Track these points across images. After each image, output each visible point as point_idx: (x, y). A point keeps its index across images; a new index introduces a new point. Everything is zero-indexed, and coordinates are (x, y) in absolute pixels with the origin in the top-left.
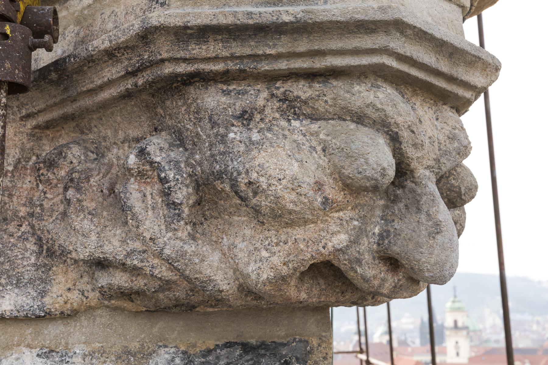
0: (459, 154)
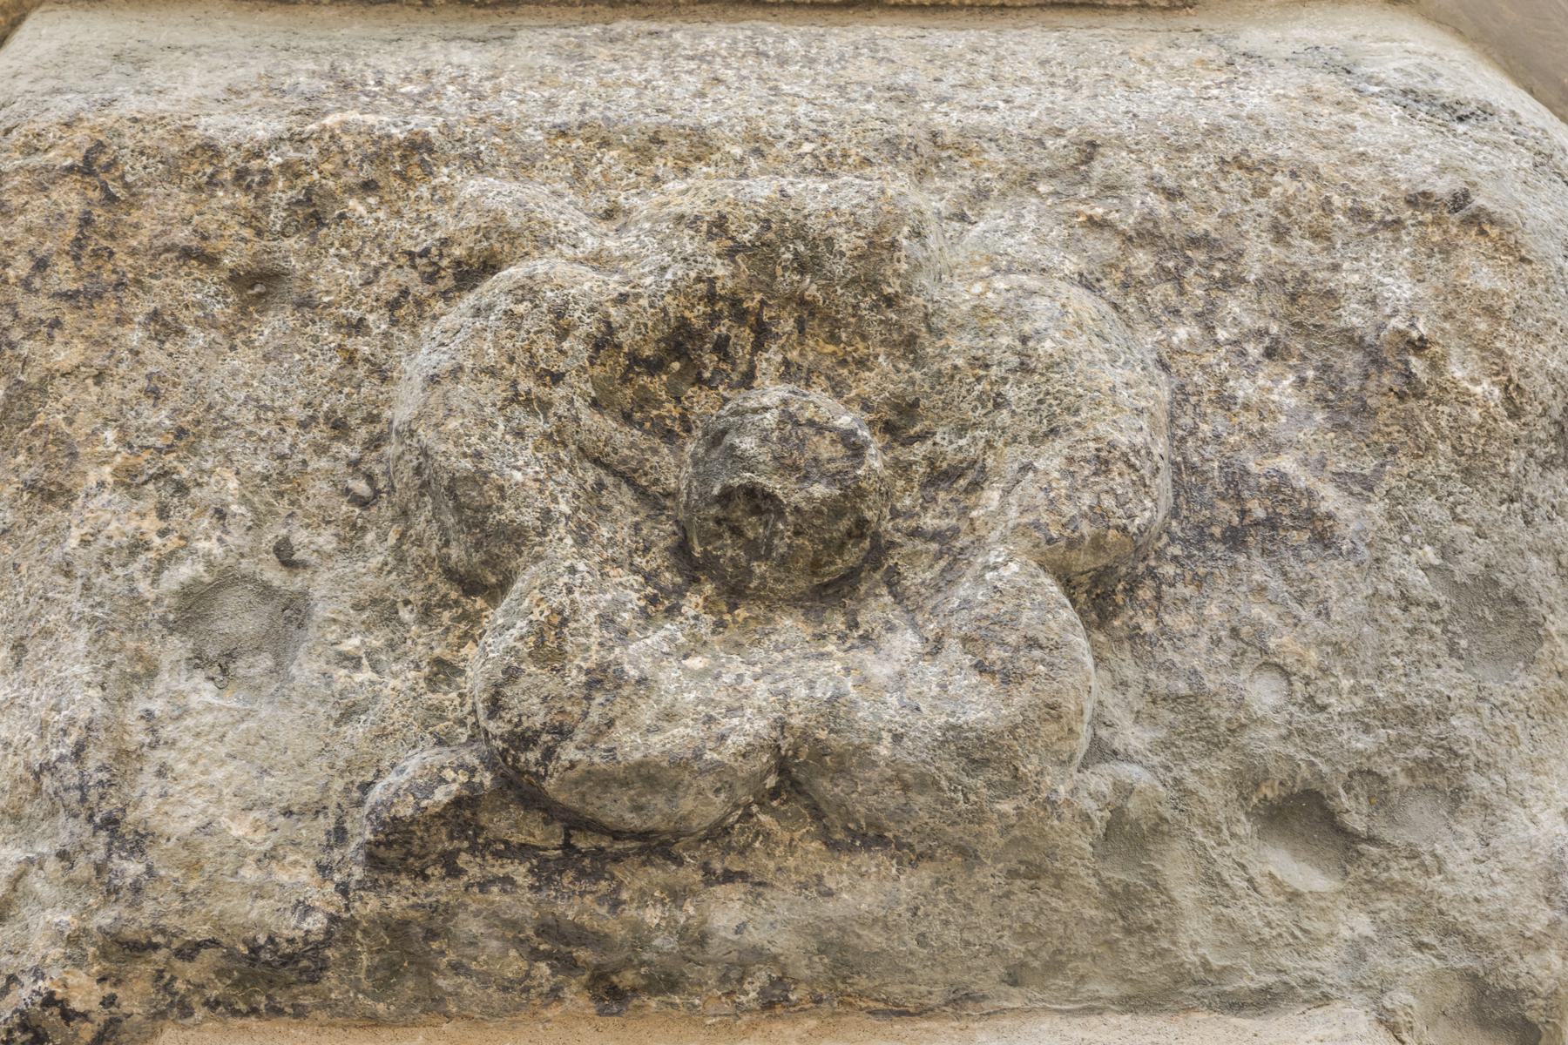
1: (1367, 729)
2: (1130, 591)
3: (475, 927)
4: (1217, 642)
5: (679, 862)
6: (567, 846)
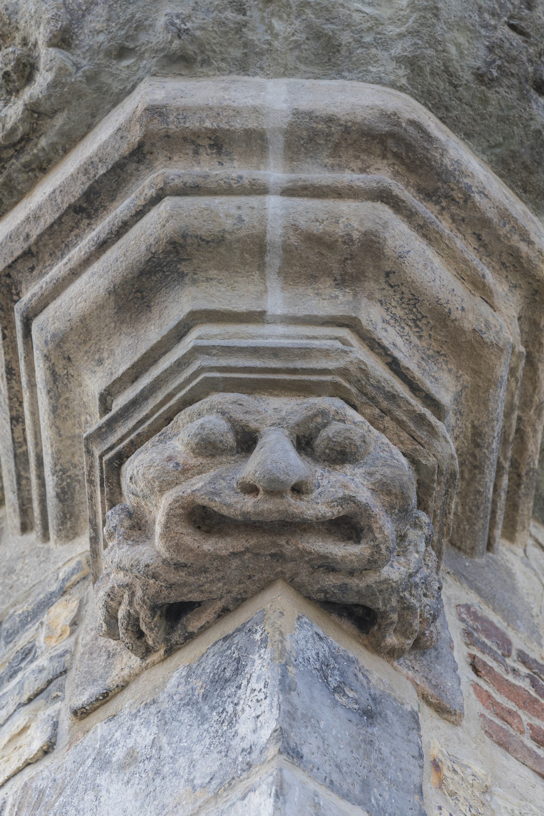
0: (306, 409)
1: (123, 29)
2: (72, 39)
3: (15, 175)
4: (89, 36)
5: (32, 139)
6: (16, 151)
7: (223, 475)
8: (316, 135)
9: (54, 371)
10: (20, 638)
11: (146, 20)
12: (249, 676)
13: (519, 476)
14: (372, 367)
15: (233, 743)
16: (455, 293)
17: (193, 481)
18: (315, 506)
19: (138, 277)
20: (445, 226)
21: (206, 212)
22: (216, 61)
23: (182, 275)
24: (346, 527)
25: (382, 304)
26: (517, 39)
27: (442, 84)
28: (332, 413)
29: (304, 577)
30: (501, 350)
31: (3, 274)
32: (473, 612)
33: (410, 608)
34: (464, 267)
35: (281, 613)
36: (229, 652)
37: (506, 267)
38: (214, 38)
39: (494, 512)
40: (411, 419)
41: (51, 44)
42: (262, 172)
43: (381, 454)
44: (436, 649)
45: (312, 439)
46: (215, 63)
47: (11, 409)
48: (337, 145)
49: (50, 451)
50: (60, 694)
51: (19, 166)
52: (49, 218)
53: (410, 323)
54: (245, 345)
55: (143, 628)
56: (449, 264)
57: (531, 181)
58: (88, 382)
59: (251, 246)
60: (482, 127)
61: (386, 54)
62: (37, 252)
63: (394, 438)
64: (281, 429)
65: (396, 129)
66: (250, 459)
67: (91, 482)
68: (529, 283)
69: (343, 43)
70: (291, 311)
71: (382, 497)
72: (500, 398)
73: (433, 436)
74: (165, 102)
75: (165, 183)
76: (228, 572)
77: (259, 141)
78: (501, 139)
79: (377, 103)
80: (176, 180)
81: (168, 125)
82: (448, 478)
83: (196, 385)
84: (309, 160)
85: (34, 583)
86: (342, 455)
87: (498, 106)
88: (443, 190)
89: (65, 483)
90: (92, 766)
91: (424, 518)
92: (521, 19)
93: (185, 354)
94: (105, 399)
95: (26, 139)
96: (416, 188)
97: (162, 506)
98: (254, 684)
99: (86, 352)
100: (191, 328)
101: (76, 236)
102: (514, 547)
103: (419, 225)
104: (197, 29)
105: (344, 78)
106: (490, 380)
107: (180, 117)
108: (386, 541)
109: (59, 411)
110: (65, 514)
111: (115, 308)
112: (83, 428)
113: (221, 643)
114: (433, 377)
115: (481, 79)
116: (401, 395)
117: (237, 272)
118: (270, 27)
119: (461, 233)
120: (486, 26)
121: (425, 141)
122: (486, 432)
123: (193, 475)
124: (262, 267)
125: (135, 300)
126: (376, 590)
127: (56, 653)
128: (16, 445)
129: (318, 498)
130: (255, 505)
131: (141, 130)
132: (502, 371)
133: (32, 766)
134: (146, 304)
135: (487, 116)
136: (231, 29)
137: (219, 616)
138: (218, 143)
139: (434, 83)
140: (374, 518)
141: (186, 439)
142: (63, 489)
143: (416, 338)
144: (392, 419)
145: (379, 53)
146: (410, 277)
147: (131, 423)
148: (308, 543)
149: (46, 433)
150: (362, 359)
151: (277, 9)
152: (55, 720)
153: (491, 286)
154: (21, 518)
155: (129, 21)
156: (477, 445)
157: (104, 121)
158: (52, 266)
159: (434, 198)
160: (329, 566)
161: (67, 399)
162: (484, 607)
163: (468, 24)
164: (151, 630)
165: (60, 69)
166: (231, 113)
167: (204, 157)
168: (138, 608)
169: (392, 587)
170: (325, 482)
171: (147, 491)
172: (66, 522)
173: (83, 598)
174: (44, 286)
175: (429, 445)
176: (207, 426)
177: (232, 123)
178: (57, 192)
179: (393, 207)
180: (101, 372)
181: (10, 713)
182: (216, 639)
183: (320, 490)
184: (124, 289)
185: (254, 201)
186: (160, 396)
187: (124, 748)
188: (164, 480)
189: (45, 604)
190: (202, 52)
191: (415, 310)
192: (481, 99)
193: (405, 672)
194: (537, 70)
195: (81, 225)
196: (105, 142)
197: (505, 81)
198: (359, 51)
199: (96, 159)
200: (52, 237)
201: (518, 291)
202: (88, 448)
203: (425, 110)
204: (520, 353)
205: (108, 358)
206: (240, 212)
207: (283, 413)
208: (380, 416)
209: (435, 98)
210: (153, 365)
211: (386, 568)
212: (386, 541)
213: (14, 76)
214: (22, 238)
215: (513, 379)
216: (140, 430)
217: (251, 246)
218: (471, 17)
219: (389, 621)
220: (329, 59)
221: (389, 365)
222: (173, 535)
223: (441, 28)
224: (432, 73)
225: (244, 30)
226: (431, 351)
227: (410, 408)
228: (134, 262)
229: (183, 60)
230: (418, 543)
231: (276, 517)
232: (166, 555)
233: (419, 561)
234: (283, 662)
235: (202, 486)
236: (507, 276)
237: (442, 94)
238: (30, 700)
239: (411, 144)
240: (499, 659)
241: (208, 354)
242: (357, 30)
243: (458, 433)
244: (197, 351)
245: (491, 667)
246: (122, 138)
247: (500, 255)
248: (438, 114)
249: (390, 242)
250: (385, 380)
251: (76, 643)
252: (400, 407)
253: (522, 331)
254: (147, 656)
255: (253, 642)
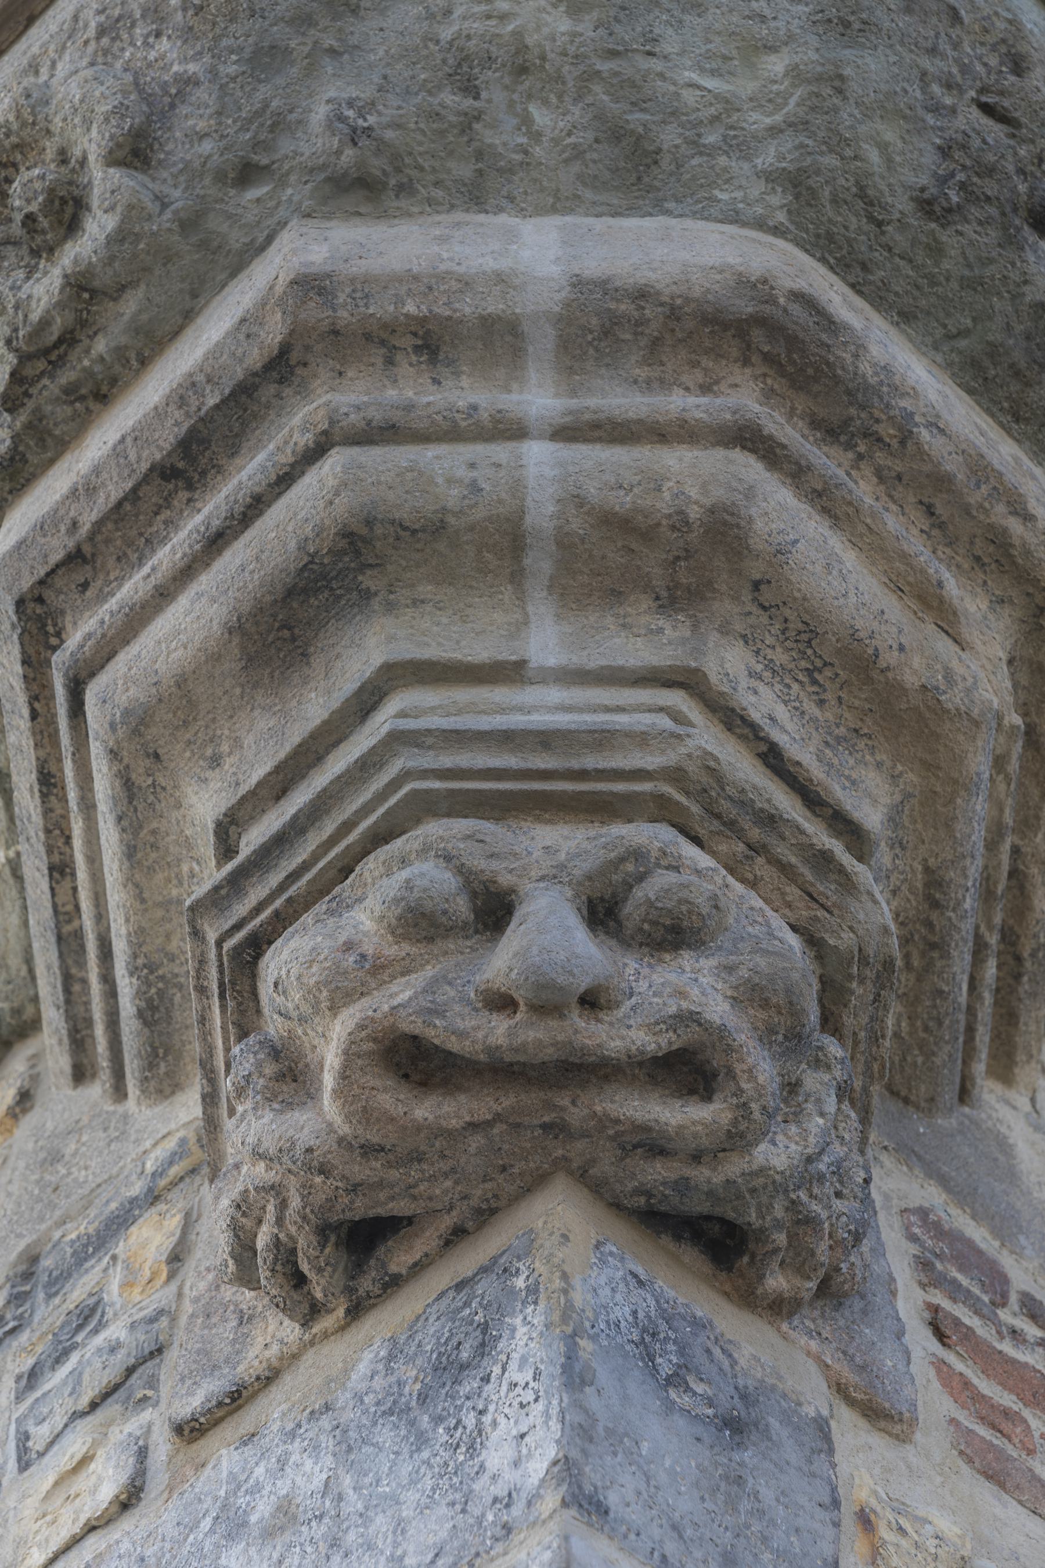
0: (604, 848)
1: (248, 130)
2: (152, 150)
3: (50, 408)
4: (183, 143)
5: (81, 341)
6: (50, 362)
7: (450, 976)
8: (616, 324)
9: (128, 780)
10: (74, 1286)
11: (291, 112)
12: (504, 1359)
13: (1018, 959)
14: (730, 764)
15: (476, 1487)
16: (885, 617)
17: (394, 988)
18: (624, 1032)
19: (284, 599)
20: (864, 491)
21: (409, 476)
22: (424, 186)
23: (367, 595)
24: (685, 1069)
25: (746, 642)
26: (995, 131)
27: (854, 220)
28: (654, 854)
29: (605, 1166)
30: (977, 724)
31: (30, 596)
32: (934, 1222)
33: (810, 1222)
34: (902, 567)
35: (563, 1236)
36: (467, 1311)
37: (983, 565)
38: (420, 144)
39: (970, 1030)
40: (806, 861)
41: (112, 160)
42: (515, 397)
43: (750, 929)
44: (863, 1297)
45: (616, 903)
46: (423, 191)
47: (50, 851)
48: (656, 342)
49: (123, 931)
50: (149, 1393)
51: (57, 391)
52: (114, 490)
53: (801, 677)
54: (486, 727)
55: (305, 1267)
56: (873, 563)
57: (1029, 400)
58: (193, 799)
59: (497, 536)
60: (933, 299)
61: (746, 166)
62: (93, 555)
63: (773, 897)
64: (558, 887)
65: (767, 309)
66: (501, 945)
67: (202, 990)
68: (1028, 594)
69: (665, 147)
70: (575, 659)
71: (752, 1012)
72: (976, 814)
73: (848, 891)
74: (328, 268)
75: (332, 422)
76: (463, 1160)
77: (508, 338)
78: (969, 321)
79: (731, 260)
80: (352, 416)
81: (335, 310)
82: (878, 971)
83: (396, 804)
84: (603, 371)
85: (99, 1180)
86: (674, 934)
87: (961, 260)
88: (859, 422)
89: (153, 990)
90: (212, 1531)
91: (834, 1049)
92: (1001, 93)
93: (374, 747)
94: (226, 832)
95: (68, 339)
96: (807, 420)
97: (335, 1037)
98: (514, 1374)
99: (189, 743)
100: (386, 694)
101: (166, 523)
102: (1012, 1095)
103: (815, 491)
104: (388, 126)
105: (668, 213)
106: (956, 782)
107: (358, 295)
108: (761, 1096)
109: (139, 855)
110: (154, 1049)
111: (241, 659)
112: (186, 886)
113: (451, 1294)
114: (848, 778)
115: (928, 208)
116: (785, 816)
117: (471, 587)
118: (527, 120)
119: (895, 502)
120: (936, 109)
121: (824, 330)
122: (951, 880)
123: (393, 977)
124: (517, 577)
125: (279, 643)
126: (743, 1188)
127: (142, 1314)
128: (61, 918)
129: (629, 1017)
130: (511, 1033)
131: (284, 321)
132: (980, 764)
133: (99, 1533)
134: (300, 651)
135: (942, 278)
136: (452, 126)
137: (448, 1243)
138: (430, 342)
139: (839, 219)
140: (737, 1052)
141: (378, 909)
142: (150, 1001)
143: (813, 705)
144: (769, 862)
145: (733, 164)
146: (799, 590)
147: (275, 879)
148: (612, 1102)
149: (116, 897)
150: (709, 749)
151: (539, 85)
152: (141, 1443)
153: (955, 601)
154: (72, 1057)
155: (258, 114)
156: (935, 905)
157: (214, 303)
158: (121, 580)
159: (843, 438)
160: (653, 1145)
161: (154, 832)
162: (954, 1211)
163: (902, 105)
164: (320, 1270)
165: (130, 207)
166: (455, 285)
167: (404, 368)
168: (293, 1229)
169: (774, 1182)
170: (642, 986)
171: (306, 1009)
172: (158, 1065)
173: (192, 1208)
174: (107, 619)
175: (840, 908)
176: (418, 883)
177: (457, 305)
178: (129, 440)
179: (764, 457)
180: (216, 781)
181: (56, 1431)
182: (442, 1287)
183: (633, 1000)
184: (257, 623)
185: (500, 451)
186: (329, 827)
187: (272, 1497)
188: (338, 988)
189: (120, 1222)
190: (398, 170)
191: (809, 652)
192: (928, 246)
193: (803, 1342)
194: (1036, 189)
195: (176, 503)
196: (217, 345)
197: (975, 212)
198: (695, 162)
199: (201, 378)
200: (120, 525)
201: (1007, 610)
202: (194, 927)
203: (823, 270)
204: (1013, 727)
205: (230, 754)
206: (475, 474)
207: (562, 856)
208: (747, 857)
209: (841, 248)
210: (315, 765)
211: (762, 1147)
212: (761, 1096)
213: (44, 222)
214: (63, 529)
215: (1001, 777)
216: (291, 891)
217: (497, 536)
218: (906, 91)
219: (770, 1247)
220: (639, 179)
221: (763, 757)
222: (356, 1091)
223: (850, 115)
224: (834, 201)
225: (476, 126)
226: (842, 729)
227: (803, 839)
228: (277, 572)
229: (363, 185)
230: (824, 1096)
231: (550, 1054)
232: (344, 1129)
233: (825, 1132)
234: (569, 1330)
235: (410, 999)
236: (985, 582)
237: (855, 239)
238: (94, 1406)
239: (797, 337)
240: (985, 1311)
241: (417, 746)
242: (689, 122)
243: (898, 883)
244: (396, 740)
245: (969, 1328)
246: (248, 336)
247: (972, 543)
248: (848, 277)
249: (759, 524)
250: (755, 787)
251: (180, 1295)
252: (784, 839)
253: (1016, 685)
254: (312, 1319)
255: (512, 1292)
